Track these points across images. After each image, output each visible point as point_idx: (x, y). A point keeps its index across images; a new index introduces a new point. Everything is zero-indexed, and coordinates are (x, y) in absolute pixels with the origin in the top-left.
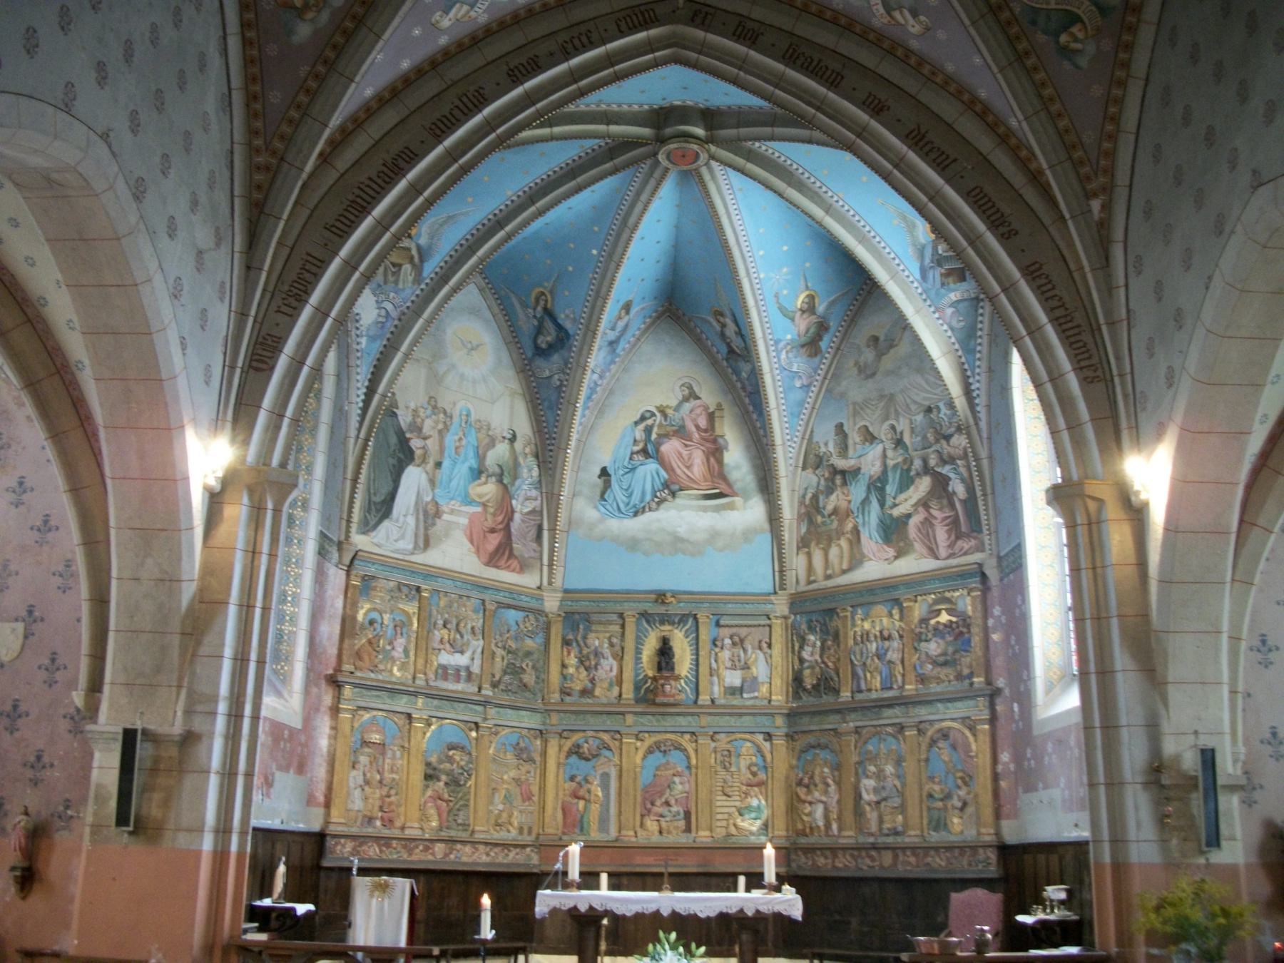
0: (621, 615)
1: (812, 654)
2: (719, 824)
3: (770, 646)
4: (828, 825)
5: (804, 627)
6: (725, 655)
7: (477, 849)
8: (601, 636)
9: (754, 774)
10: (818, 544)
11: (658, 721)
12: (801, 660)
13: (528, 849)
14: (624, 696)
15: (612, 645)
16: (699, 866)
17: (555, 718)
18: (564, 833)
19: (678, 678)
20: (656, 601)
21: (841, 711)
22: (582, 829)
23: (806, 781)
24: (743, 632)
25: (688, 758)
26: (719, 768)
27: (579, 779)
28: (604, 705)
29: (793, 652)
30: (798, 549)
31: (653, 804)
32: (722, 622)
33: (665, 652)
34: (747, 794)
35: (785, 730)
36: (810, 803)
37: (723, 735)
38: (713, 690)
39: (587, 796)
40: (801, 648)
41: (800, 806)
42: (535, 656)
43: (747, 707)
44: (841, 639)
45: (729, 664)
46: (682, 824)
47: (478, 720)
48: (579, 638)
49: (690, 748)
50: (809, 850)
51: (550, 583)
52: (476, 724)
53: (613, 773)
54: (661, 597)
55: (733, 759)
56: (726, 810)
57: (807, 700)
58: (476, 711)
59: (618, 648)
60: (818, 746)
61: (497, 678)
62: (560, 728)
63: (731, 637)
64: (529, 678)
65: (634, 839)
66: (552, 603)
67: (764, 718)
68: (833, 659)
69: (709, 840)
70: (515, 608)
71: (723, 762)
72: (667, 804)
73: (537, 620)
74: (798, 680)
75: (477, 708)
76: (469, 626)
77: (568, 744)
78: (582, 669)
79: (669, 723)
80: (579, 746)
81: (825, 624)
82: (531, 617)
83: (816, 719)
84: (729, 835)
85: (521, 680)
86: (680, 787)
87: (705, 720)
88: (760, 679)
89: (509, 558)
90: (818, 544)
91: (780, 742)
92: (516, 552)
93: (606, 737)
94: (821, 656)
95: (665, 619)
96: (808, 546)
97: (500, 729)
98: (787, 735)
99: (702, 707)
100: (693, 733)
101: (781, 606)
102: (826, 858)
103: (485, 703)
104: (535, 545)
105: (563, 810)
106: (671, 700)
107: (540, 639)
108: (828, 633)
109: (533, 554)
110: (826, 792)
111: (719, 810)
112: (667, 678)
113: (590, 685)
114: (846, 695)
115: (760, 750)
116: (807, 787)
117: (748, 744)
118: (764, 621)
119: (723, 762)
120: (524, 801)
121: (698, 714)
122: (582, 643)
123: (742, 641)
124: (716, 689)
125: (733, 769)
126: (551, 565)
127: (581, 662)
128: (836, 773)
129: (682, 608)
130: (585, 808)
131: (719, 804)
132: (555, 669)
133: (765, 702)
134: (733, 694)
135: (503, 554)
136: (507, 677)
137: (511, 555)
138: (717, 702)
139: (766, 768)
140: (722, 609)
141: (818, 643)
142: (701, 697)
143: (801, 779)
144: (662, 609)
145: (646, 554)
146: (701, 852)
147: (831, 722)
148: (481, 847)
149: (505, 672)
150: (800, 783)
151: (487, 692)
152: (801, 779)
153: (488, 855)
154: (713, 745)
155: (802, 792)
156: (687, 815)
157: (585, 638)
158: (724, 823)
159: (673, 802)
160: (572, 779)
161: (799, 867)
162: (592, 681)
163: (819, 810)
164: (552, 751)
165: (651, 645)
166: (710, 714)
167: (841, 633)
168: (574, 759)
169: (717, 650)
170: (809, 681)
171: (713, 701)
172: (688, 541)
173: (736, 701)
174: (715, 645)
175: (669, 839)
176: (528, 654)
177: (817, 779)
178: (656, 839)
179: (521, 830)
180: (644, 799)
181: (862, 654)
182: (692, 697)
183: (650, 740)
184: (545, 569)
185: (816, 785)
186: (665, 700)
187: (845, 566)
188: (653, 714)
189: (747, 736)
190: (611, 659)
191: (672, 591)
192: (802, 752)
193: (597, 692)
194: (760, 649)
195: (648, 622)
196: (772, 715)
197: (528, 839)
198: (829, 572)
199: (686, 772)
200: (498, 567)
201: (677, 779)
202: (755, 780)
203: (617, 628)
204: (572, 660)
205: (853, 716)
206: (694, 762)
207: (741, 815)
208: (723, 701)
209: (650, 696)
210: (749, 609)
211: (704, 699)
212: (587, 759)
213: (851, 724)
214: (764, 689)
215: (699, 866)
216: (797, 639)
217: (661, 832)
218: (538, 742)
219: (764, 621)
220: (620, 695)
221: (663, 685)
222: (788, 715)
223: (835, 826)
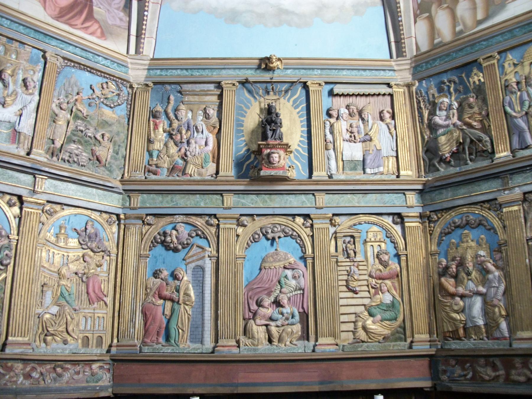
0: (219, 85)
1: (448, 117)
2: (344, 327)
3: (393, 117)
4: (491, 325)
5: (433, 91)
6: (342, 126)
7: (11, 369)
8: (195, 107)
9: (385, 265)
10: (440, 5)
11: (265, 201)
12: (433, 127)
13: (95, 366)
14: (221, 173)
15: (207, 116)
16: (321, 383)
17: (138, 200)
18: (144, 343)
19: (286, 147)
20: (259, 67)
21: (503, 174)
22: (168, 338)
23: (453, 268)
24: (361, 102)
25: (303, 247)
26: (341, 258)
27: (166, 273)
28: (197, 182)
29: (422, 121)
30: (416, 16)
31: (259, 304)
32: (336, 91)
33: (270, 120)
34: (378, 290)
35: (418, 210)
36: (462, 297)
37: (343, 218)
38: (328, 166)
39: (175, 296)
40: (432, 113)
41: (448, 300)
42: (115, 128)
43: (373, 182)
44: (488, 92)
45: (347, 136)
46: (297, 328)
47: (23, 193)
48: (170, 110)
49: (305, 233)
50: (465, 359)
51: (137, 51)
52: (20, 197)
53: (209, 266)
54: (265, 64)
55: (359, 247)
56: (352, 310)
57: (443, 170)
58: (19, 182)
59: (214, 119)
60: (468, 224)
61: (58, 144)
62: (144, 212)
63: (348, 107)
64: (105, 152)
65: (235, 350)
66: (137, 74)
67: (393, 196)
68: (479, 118)
69: (333, 348)
70: (91, 70)
71: (345, 251)
72: (277, 303)
73: (119, 89)
74: (430, 153)
75: (22, 176)
76: (21, 77)
77: (153, 232)
78: (171, 144)
79: (277, 203)
80: (165, 234)
81: (462, 82)
82: (112, 86)
83: (463, 191)
84: (358, 341)
85: (93, 152)
86: (293, 283)
87: (323, 199)
88: (384, 153)
89: (86, 20)
90: (440, 5)
91: (412, 224)
92: (95, 16)
93: (199, 222)
94: (460, 119)
95: (269, 87)
96: (429, 11)
97: (58, 208)
98: (421, 216)
99: (317, 183)
100: (306, 216)
101: (401, 74)
102: (495, 368)
103: (34, 171)
104: (122, 14)
105: (144, 314)
106: (280, 173)
107: (122, 111)
108: (467, 90)
109: (118, 22)
110: (484, 281)
111: (343, 310)
112: (274, 147)
113: (181, 162)
114: (503, 154)
115: (389, 236)
116: (456, 277)
117: (375, 228)
118: (384, 90)
119: (345, 251)
120: (91, 302)
121: (312, 192)
122: (172, 115)
123: (360, 113)
124: (333, 163)
125: (359, 257)
126: (139, 36)
127: (171, 135)
128: (498, 256)
129: (291, 75)
130: (173, 311)
131: (342, 302)
132: (138, 143)
133: (394, 177)
134: (354, 169)
135: (81, 12)
136: (73, 146)
137: (90, 16)
138: (335, 178)
139: (398, 256)
140: (334, 76)
141: (456, 105)
142: (315, 174)
143: (447, 268)
144: (266, 76)
145: (247, 25)
146: (324, 365)
147: (486, 190)
148: (19, 366)
149: (69, 140)
150: (444, 272)
151: (40, 155)
152: (447, 268)
153: (28, 376)
154: (332, 230)
155: (449, 283)
156: (304, 317)
157: (176, 110)
158: (351, 327)
159: (285, 301)
160: (156, 274)
161: (453, 380)
162: (184, 158)
163: (478, 304)
164: (132, 240)
165: (253, 118)
166: (328, 192)
167: (488, 85)
168: (159, 249)
169: (333, 120)
170: (446, 148)
171: (330, 177)
172: (293, 13)
173: (358, 175)
174: (329, 115)
175: (280, 350)
176: (104, 124)
177: (470, 266)
178: (264, 349)
179: (86, 341)
180: (249, 298)
181: (522, 103)
182: (305, 174)
183: (253, 226)
184: (133, 39)
185: (468, 274)
186: (273, 173)
187: (480, 17)
188: (258, 193)
189: (373, 219)
190: (206, 132)
191: (279, 56)
192: (446, 233)
193: (191, 169)
194: (382, 119)
195: (250, 92)
196: (403, 192)
197: (94, 351)
198: (458, 29)
199: (301, 264)
200: (71, 25)
201: (289, 273)
202: (386, 272)
203: (215, 99)
204: (161, 135)
205: (518, 179)
206: (309, 251)
207: (371, 315)
208: (342, 177)
209: (254, 167)
210: (367, 76)
211: (319, 174)
212: (176, 250)
213: (517, 191)
214: (391, 163)
215: (321, 383)
216: (424, 111)
217: (270, 341)
218: (115, 228)
219: (384, 90)
220: (217, 173)
221: (269, 155)
222: (421, 192)
223: (504, 325)
